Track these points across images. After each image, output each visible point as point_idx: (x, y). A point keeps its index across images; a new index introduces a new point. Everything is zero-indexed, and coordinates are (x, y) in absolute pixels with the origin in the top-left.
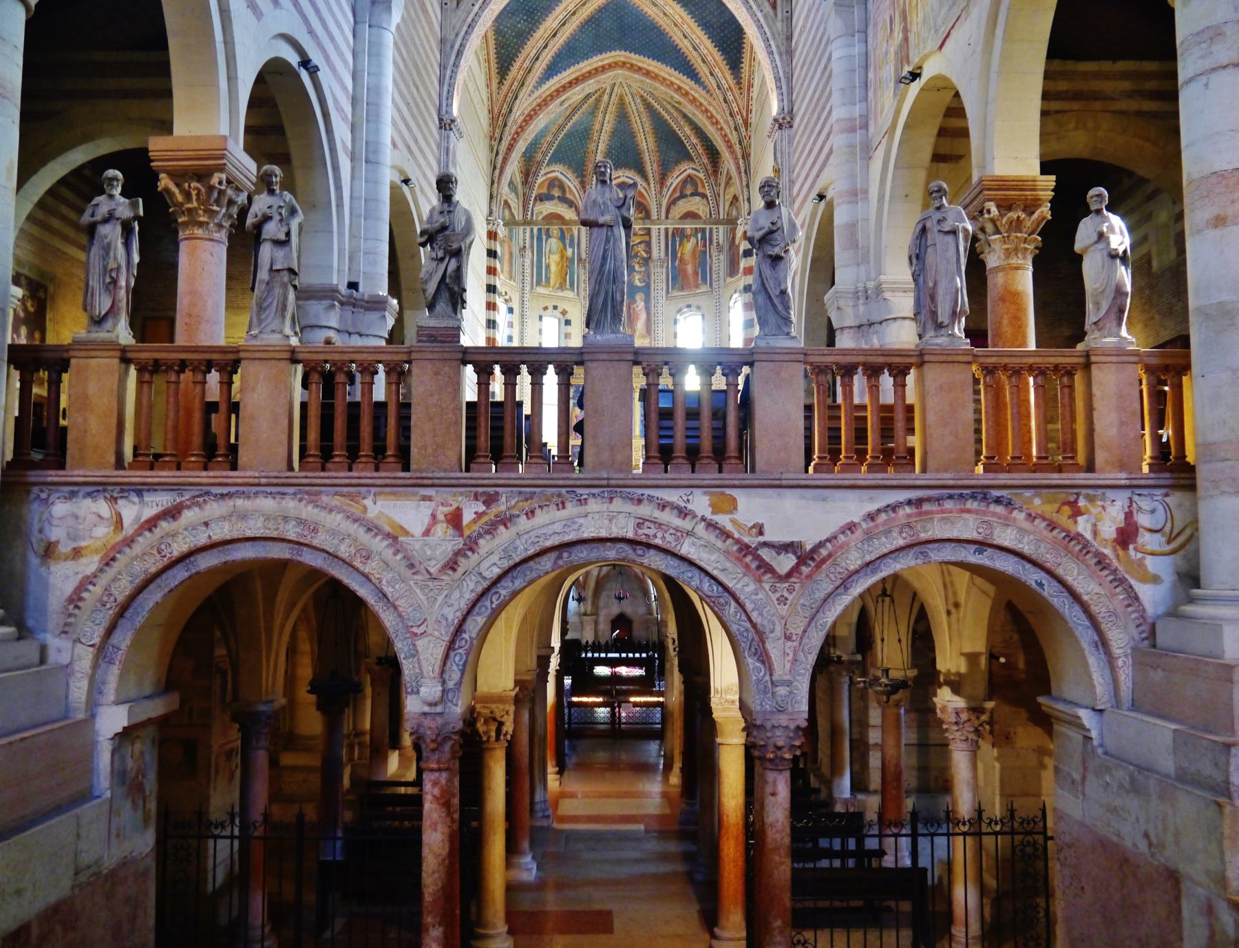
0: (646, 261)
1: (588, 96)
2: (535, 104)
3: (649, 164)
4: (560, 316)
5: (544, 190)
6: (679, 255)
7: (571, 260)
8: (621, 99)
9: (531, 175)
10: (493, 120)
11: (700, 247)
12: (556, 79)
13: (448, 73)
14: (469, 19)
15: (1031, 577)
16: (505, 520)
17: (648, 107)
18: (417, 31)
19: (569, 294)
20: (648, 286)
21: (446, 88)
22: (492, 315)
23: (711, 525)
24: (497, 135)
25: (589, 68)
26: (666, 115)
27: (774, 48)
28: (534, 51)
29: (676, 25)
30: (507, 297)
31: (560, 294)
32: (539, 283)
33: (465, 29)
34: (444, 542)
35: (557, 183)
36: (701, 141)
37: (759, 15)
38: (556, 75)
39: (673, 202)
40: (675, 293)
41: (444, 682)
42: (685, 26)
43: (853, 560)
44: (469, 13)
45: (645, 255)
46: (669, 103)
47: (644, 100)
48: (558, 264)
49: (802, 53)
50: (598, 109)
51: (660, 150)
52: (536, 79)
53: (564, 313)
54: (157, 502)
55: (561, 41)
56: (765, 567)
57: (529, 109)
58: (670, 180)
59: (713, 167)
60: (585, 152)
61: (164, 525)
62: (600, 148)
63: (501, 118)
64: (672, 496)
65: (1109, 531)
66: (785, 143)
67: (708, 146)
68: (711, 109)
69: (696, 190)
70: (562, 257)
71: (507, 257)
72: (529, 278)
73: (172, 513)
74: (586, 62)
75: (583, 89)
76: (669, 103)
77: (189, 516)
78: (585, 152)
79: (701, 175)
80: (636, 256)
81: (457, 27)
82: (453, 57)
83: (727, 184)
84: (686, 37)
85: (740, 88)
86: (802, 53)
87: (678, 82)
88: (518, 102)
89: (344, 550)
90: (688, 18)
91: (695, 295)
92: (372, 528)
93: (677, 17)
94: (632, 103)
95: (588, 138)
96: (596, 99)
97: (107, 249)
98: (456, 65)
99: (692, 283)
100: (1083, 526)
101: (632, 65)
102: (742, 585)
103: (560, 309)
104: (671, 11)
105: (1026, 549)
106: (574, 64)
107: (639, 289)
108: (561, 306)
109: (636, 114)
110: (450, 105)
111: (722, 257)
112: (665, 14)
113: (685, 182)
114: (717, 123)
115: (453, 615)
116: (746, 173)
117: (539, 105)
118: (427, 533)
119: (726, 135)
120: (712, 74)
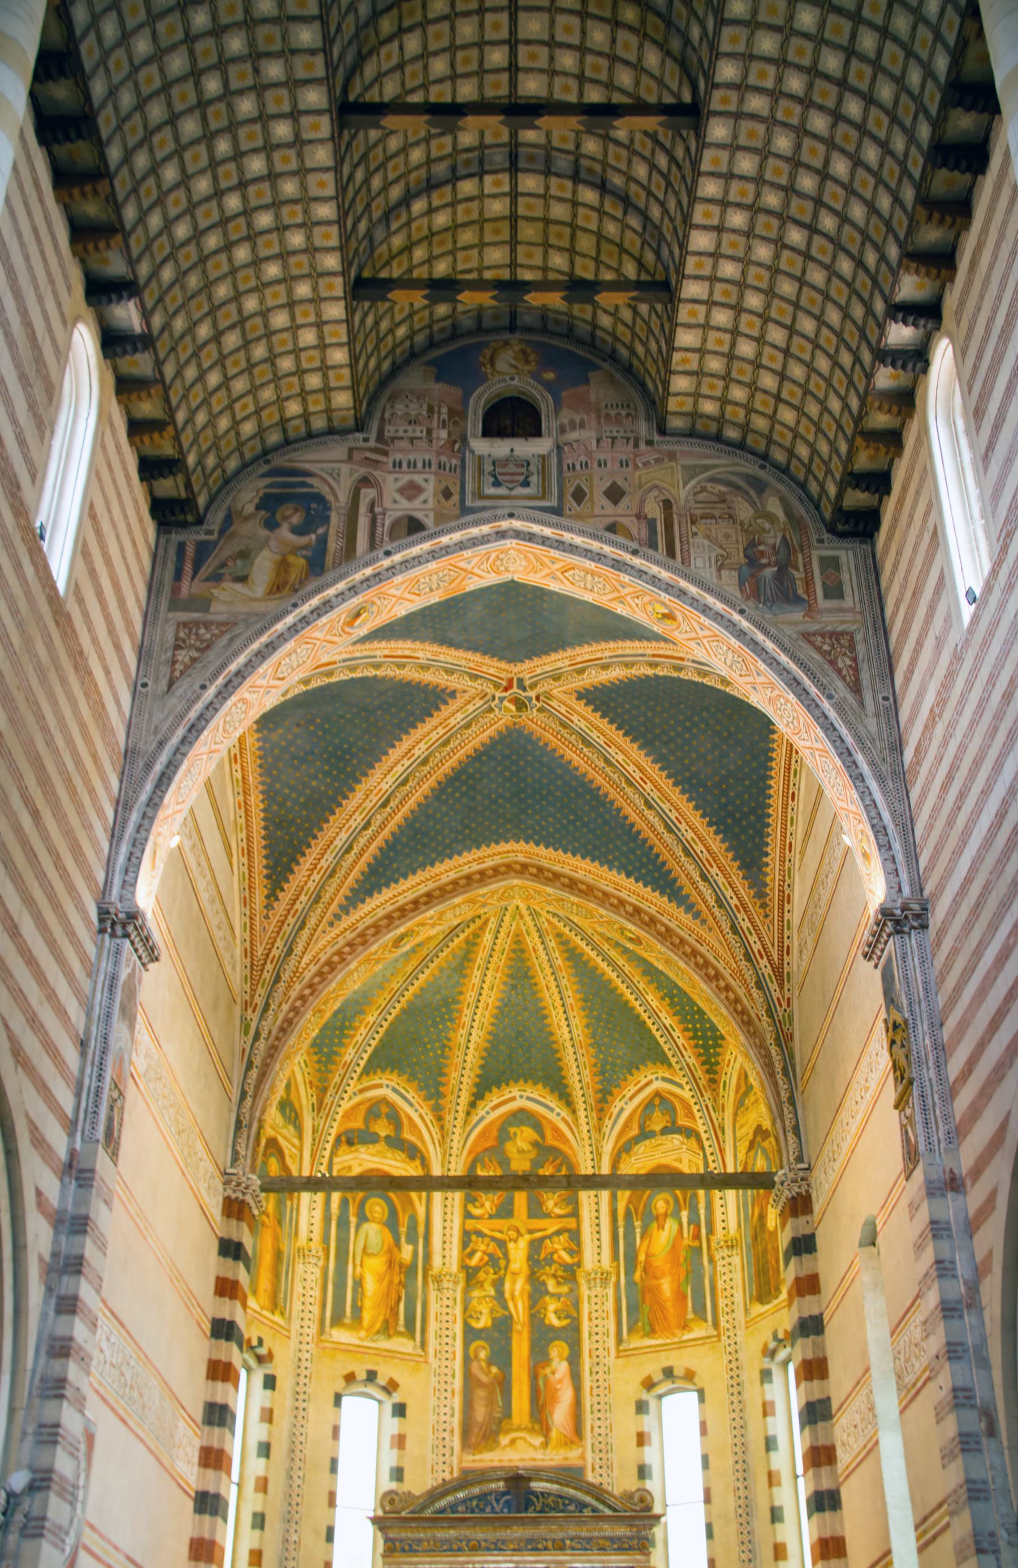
0: (570, 1273)
1: (453, 932)
2: (341, 941)
3: (574, 1070)
5: (358, 1124)
6: (642, 1257)
7: (410, 1271)
8: (518, 940)
9: (331, 1091)
10: (254, 969)
11: (687, 1240)
12: (387, 893)
13: (135, 817)
14: (193, 715)
17: (573, 956)
18: (54, 704)
19: (403, 1344)
21: (124, 849)
22: (220, 1392)
24: (259, 1001)
25: (453, 875)
26: (608, 970)
27: (865, 768)
28: (344, 836)
29: (630, 784)
30: (263, 1351)
31: (384, 1344)
32: (337, 1319)
33: (180, 732)
35: (384, 1110)
36: (683, 1021)
37: (826, 705)
38: (388, 886)
39: (625, 1148)
40: (637, 1342)
42: (648, 786)
44: (194, 702)
45: (567, 1258)
46: (617, 945)
47: (563, 942)
48: (381, 1279)
49: (939, 759)
50: (473, 961)
51: (596, 1044)
52: (345, 890)
55: (398, 818)
57: (330, 951)
58: (618, 1104)
59: (708, 1072)
60: (444, 1047)
62: (473, 1038)
63: (269, 967)
66: (914, 961)
67: (696, 1030)
68: (703, 949)
69: (674, 1122)
70: (390, 1264)
71: (267, 1260)
72: (316, 1309)
74: (448, 864)
75: (442, 914)
76: (617, 945)
78: (445, 1046)
79: (686, 1094)
80: (549, 1261)
81: (164, 728)
82: (149, 787)
83: (740, 1104)
84: (650, 807)
85: (764, 906)
86: (939, 759)
87: (633, 900)
88: (305, 933)
90: (654, 771)
91: (682, 1345)
93: (631, 768)
94: (540, 948)
95: (451, 1020)
96: (467, 941)
98: (154, 803)
99: (673, 1320)
101: (540, 869)
103: (382, 1380)
104: (620, 757)
106: (423, 866)
109: (548, 971)
110: (129, 884)
111: (736, 1260)
112: (607, 761)
113: (648, 1106)
114: (718, 976)
116: (785, 1073)
117: (350, 944)
119: (737, 1000)
120: (704, 877)
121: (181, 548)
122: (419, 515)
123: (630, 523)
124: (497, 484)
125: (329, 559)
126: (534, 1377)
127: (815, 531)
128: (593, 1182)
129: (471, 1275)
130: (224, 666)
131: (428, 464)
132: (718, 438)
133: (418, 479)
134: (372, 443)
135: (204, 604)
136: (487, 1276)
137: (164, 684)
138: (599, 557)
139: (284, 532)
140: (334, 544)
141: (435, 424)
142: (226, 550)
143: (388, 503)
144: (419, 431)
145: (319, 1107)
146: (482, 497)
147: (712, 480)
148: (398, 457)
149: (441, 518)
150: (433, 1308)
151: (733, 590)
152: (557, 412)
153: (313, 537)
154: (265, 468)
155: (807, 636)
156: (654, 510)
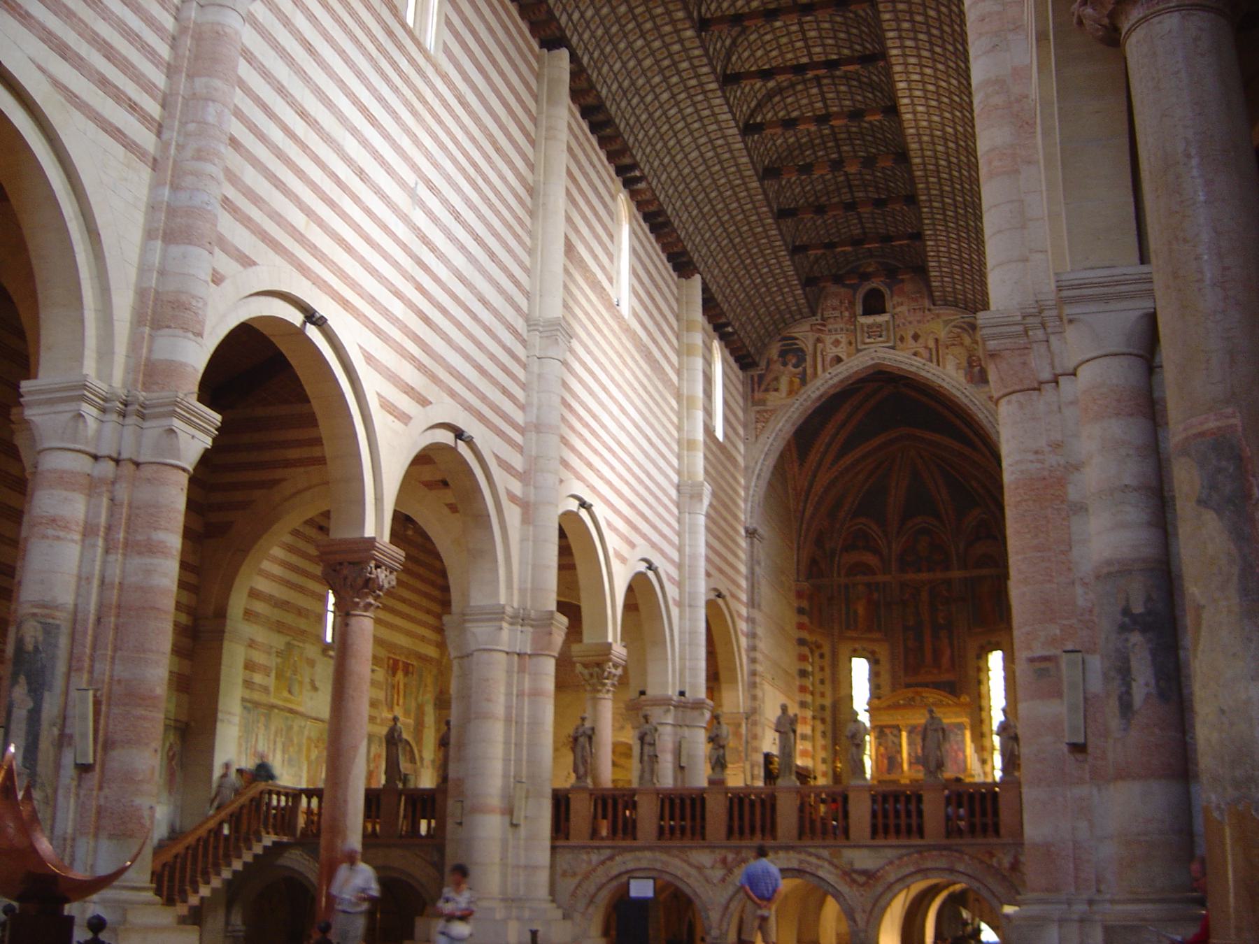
4: (869, 656)
23: (831, 863)
24: (801, 508)
33: (762, 457)
41: (720, 930)
43: (892, 878)
53: (873, 653)
56: (854, 881)
61: (608, 863)
64: (813, 850)
77: (618, 859)
89: (679, 873)
97: (583, 748)
100: (995, 862)
105: (970, 872)
115: (723, 901)
118: (713, 867)
121: (752, 377)
122: (840, 355)
123: (922, 350)
124: (869, 337)
125: (808, 379)
130: (774, 429)
131: (842, 329)
132: (957, 306)
133: (838, 337)
134: (819, 322)
135: (763, 402)
137: (754, 439)
139: (790, 367)
140: (809, 371)
141: (843, 309)
142: (770, 377)
143: (829, 351)
144: (837, 314)
147: (955, 327)
148: (830, 327)
149: (849, 355)
152: (892, 297)
153: (801, 369)
154: (779, 337)
156: (931, 344)
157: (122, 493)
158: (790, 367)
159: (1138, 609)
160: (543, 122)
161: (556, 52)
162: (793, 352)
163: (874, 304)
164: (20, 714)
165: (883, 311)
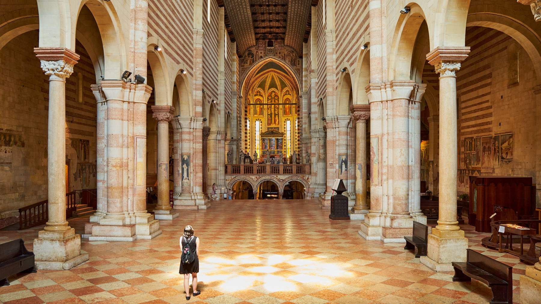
0: (278, 108)
15: (301, 182)
16: (260, 178)
20: (279, 114)
34: (256, 179)
39: (284, 95)
40: (284, 116)
54: (235, 176)
64: (273, 176)
65: (306, 178)
73: (235, 177)
91: (289, 116)
92: (251, 178)
100: (305, 178)
102: (278, 182)
107: (277, 114)
108: (260, 119)
115: (257, 185)
126: (274, 119)
127: (298, 57)
128: (281, 104)
129: (268, 109)
135: (243, 66)
136: (270, 109)
138: (278, 60)
139: (250, 58)
140: (255, 59)
142: (245, 60)
145: (252, 93)
146: (268, 53)
149: (264, 56)
150: (264, 112)
151: (290, 64)
155: (296, 69)
156: (283, 55)
157: (194, 134)
158: (250, 58)
159: (344, 160)
160: (219, 24)
161: (222, 8)
162: (250, 54)
163: (270, 44)
164: (185, 169)
165: (272, 46)
